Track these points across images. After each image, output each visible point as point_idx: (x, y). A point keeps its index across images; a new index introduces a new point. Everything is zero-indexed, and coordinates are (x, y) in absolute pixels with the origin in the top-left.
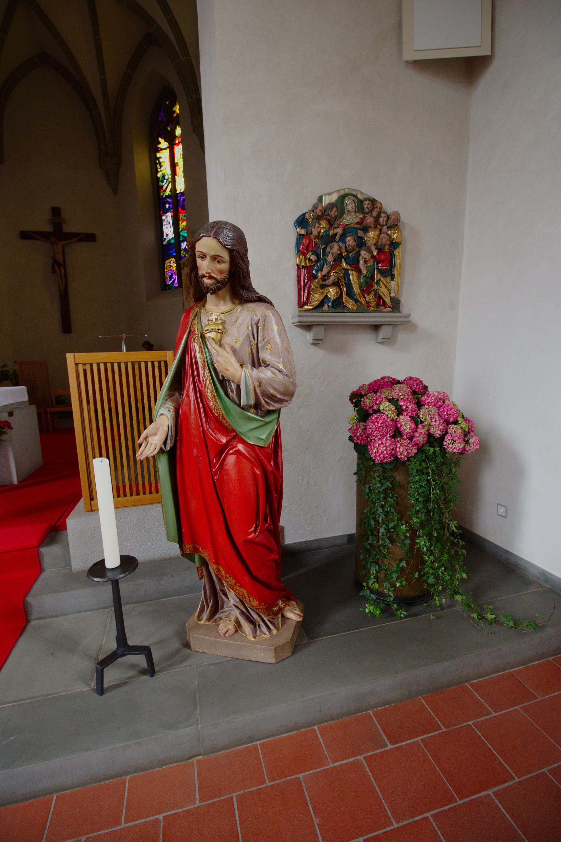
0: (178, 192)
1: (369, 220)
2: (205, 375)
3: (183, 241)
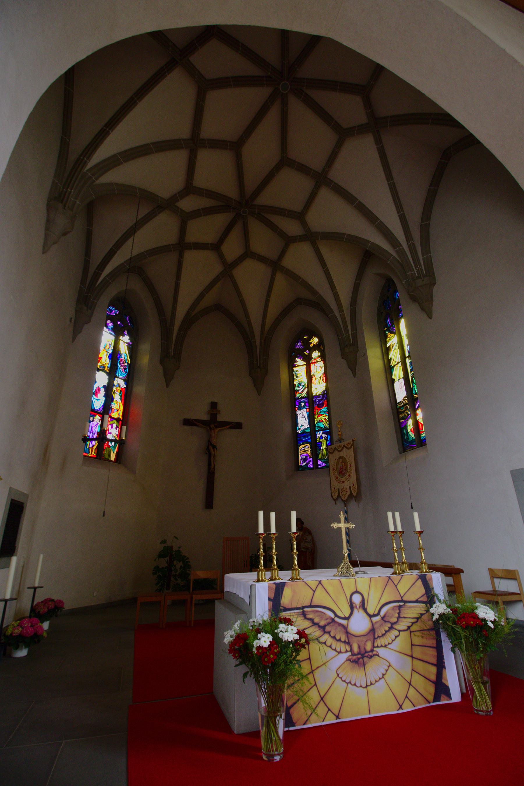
0: (313, 395)
3: (318, 431)
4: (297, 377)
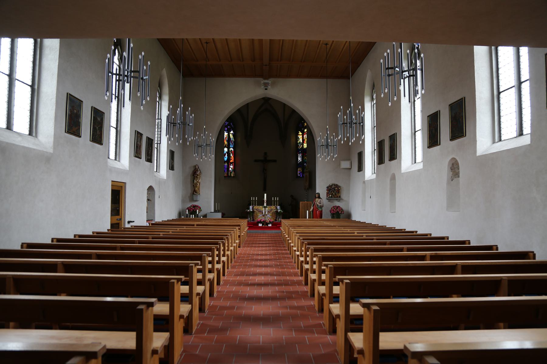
1: (336, 187)
2: (316, 204)
4: (299, 140)
